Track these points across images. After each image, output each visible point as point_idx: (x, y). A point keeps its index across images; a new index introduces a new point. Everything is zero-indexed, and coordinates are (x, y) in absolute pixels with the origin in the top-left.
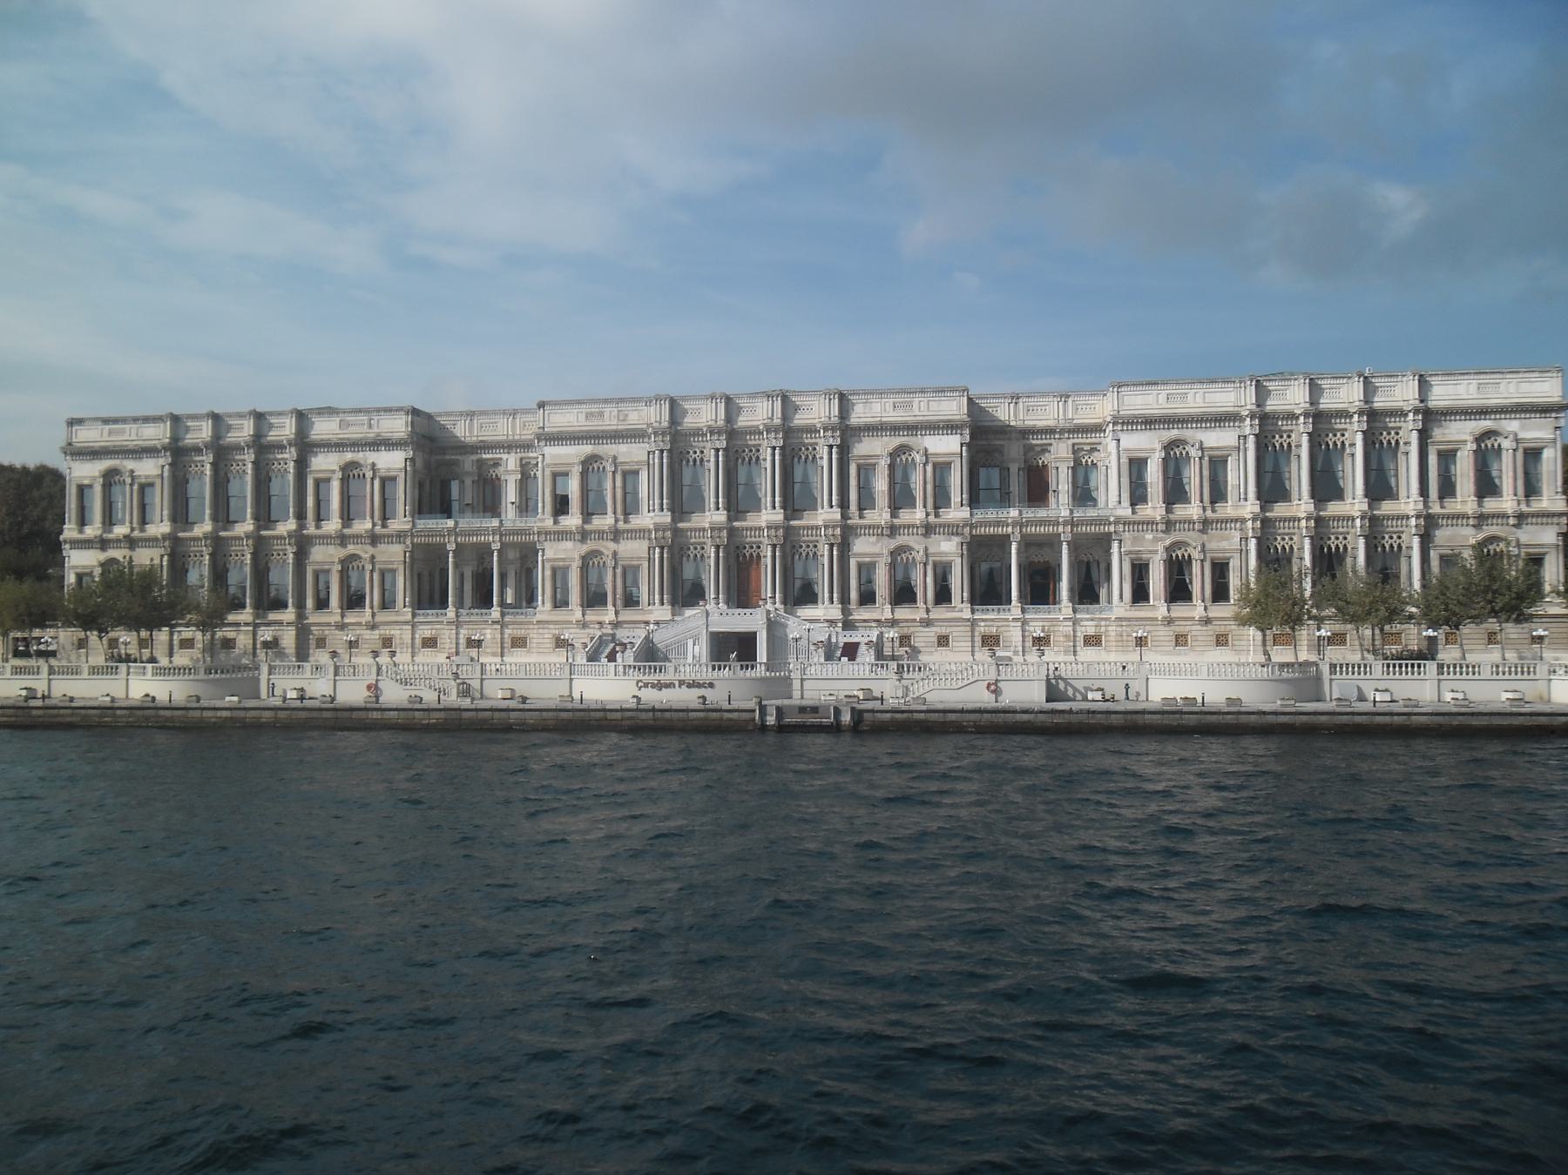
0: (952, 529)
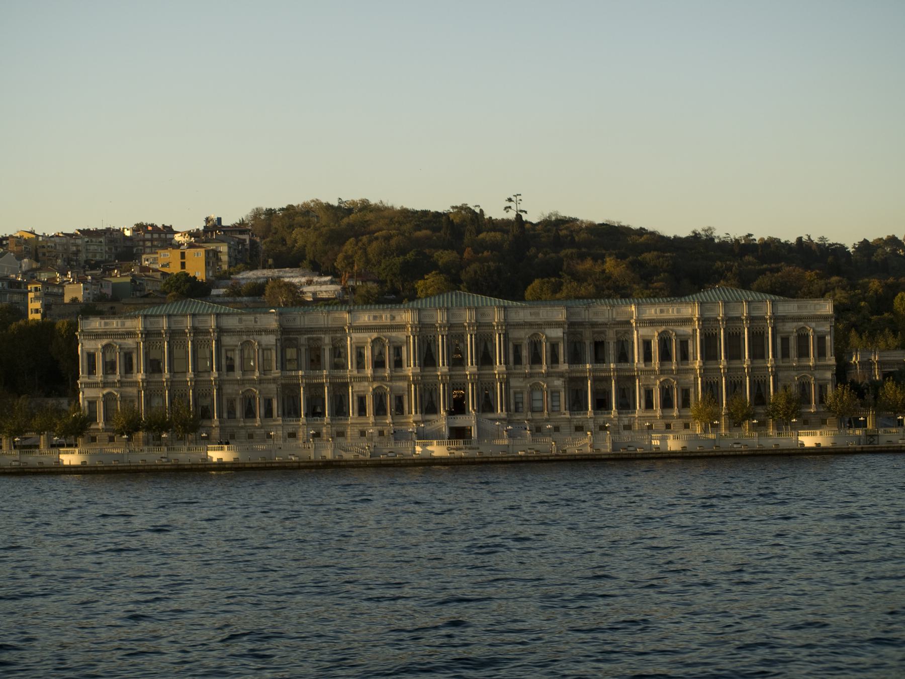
0: (561, 375)
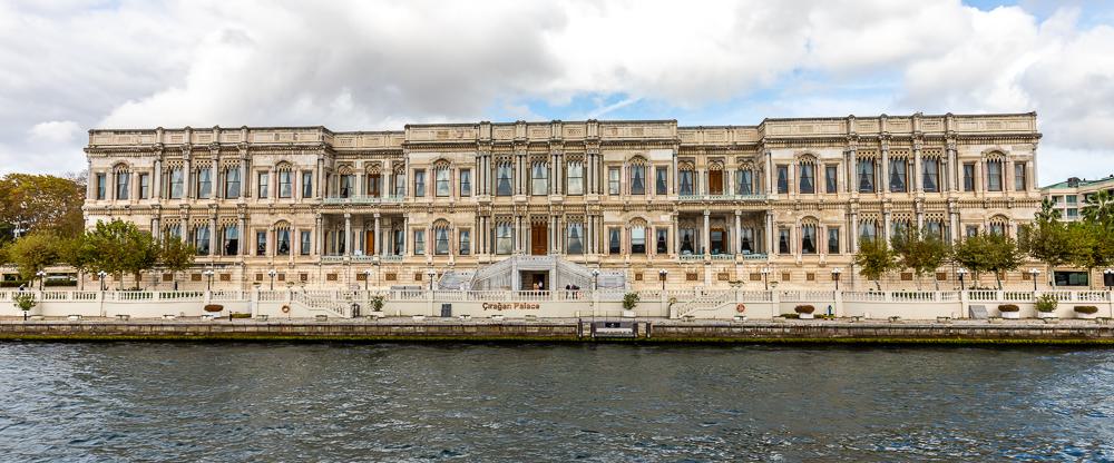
0: (668, 208)
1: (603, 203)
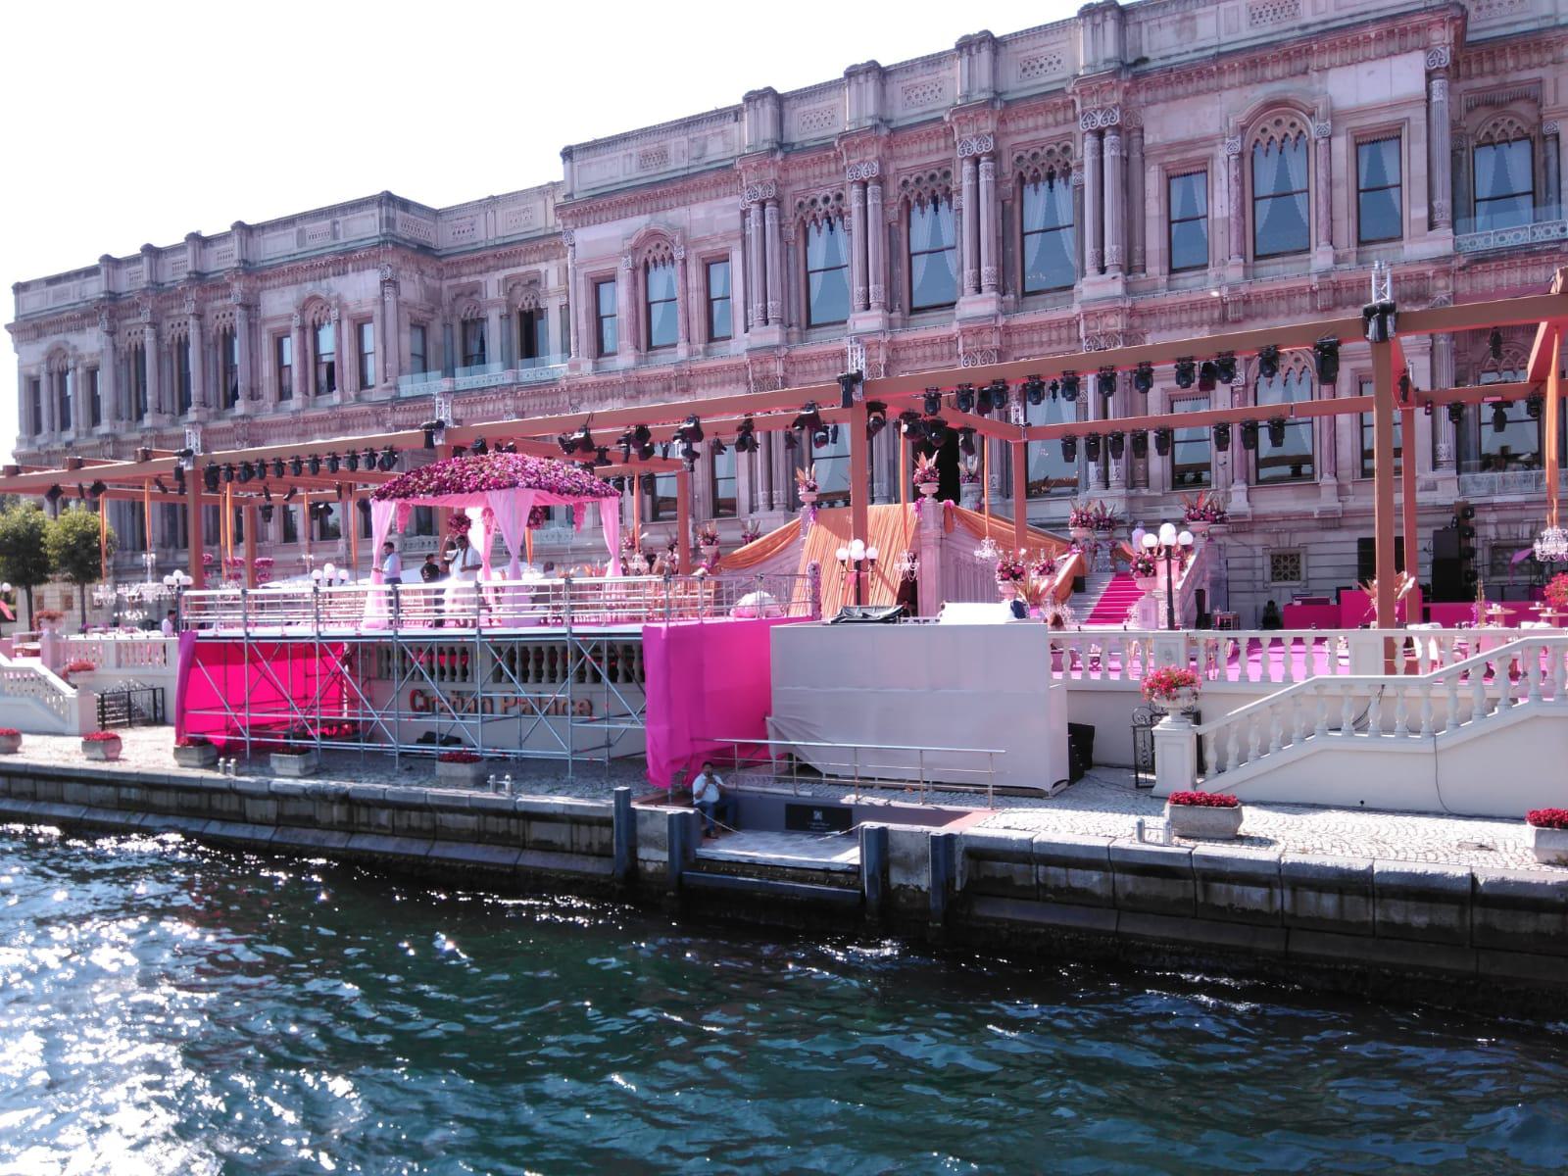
1: (1143, 304)
